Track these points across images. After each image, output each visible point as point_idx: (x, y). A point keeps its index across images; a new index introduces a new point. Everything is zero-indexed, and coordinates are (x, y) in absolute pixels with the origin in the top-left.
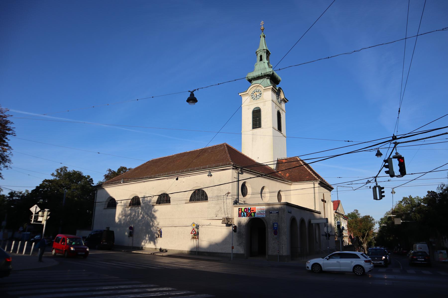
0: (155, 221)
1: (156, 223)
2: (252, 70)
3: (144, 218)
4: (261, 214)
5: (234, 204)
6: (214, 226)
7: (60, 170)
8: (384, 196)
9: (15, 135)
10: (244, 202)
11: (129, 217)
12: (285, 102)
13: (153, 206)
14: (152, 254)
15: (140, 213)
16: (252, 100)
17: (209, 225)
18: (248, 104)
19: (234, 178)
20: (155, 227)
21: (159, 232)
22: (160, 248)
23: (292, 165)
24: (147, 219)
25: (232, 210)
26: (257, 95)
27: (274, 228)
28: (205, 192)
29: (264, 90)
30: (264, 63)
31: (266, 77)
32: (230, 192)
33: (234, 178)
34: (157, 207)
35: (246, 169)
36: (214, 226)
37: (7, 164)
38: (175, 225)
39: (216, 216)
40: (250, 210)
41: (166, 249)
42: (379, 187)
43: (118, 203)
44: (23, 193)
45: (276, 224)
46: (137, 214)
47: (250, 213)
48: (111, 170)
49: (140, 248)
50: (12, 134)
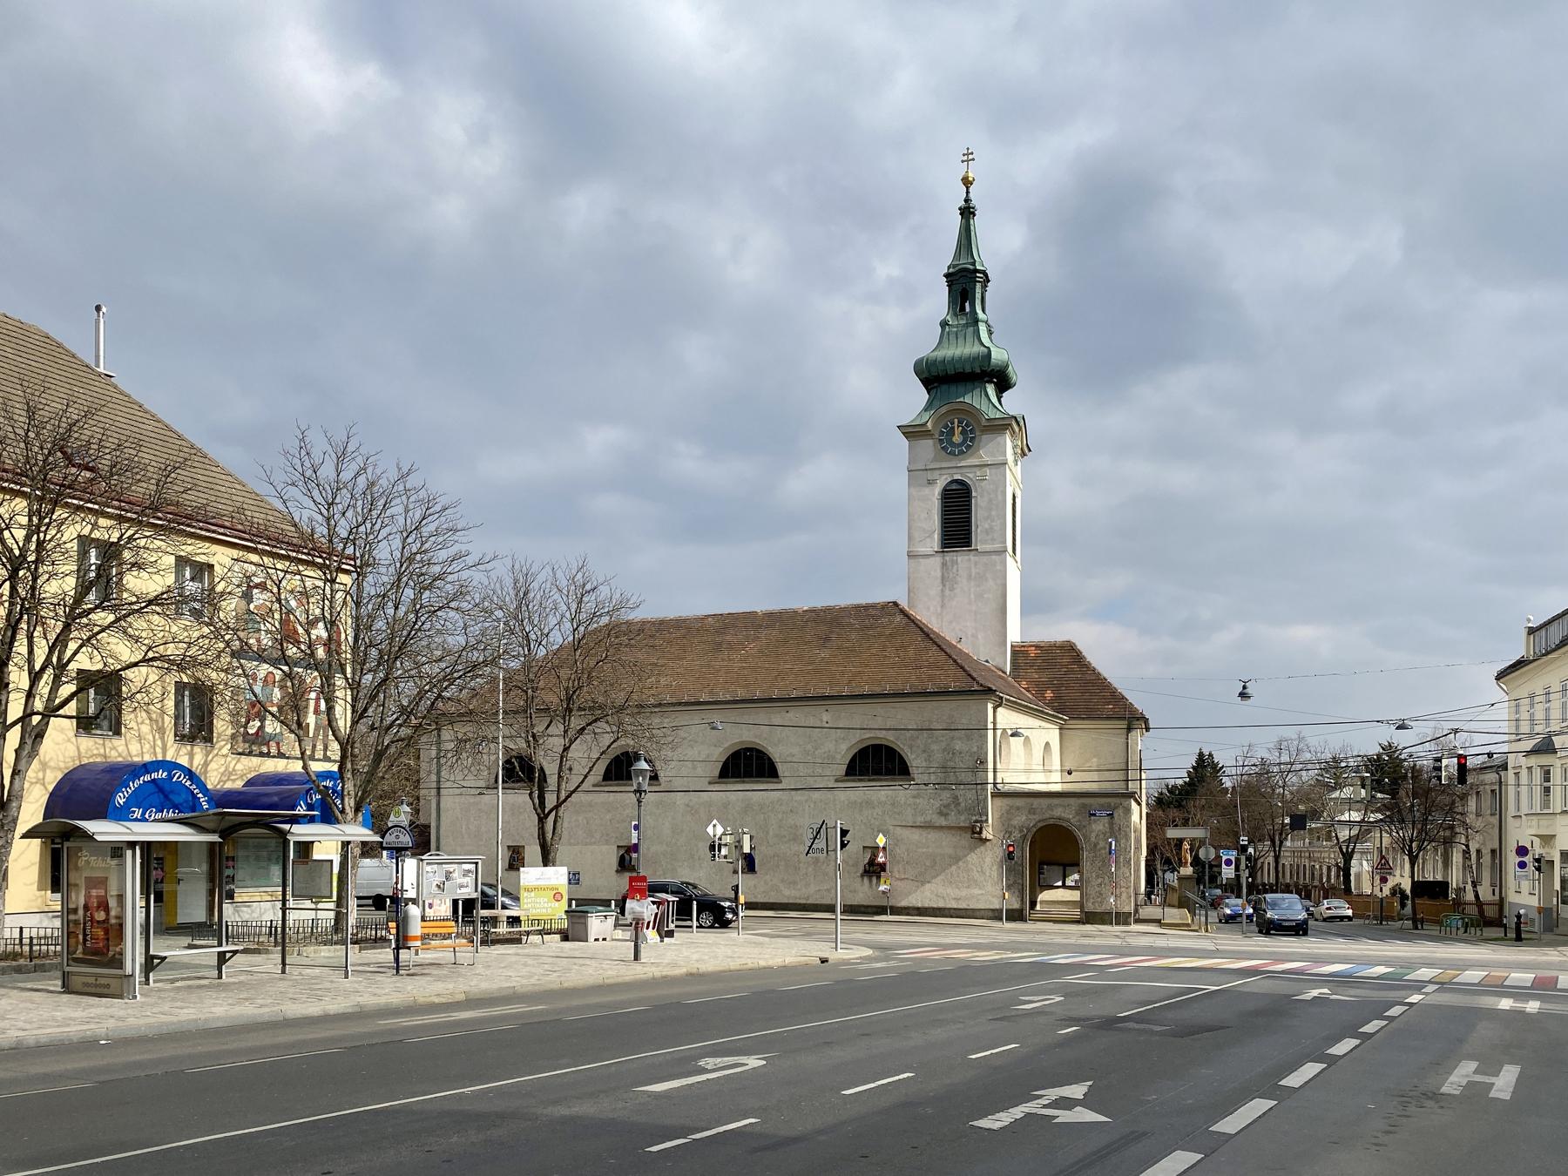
18: (928, 468)
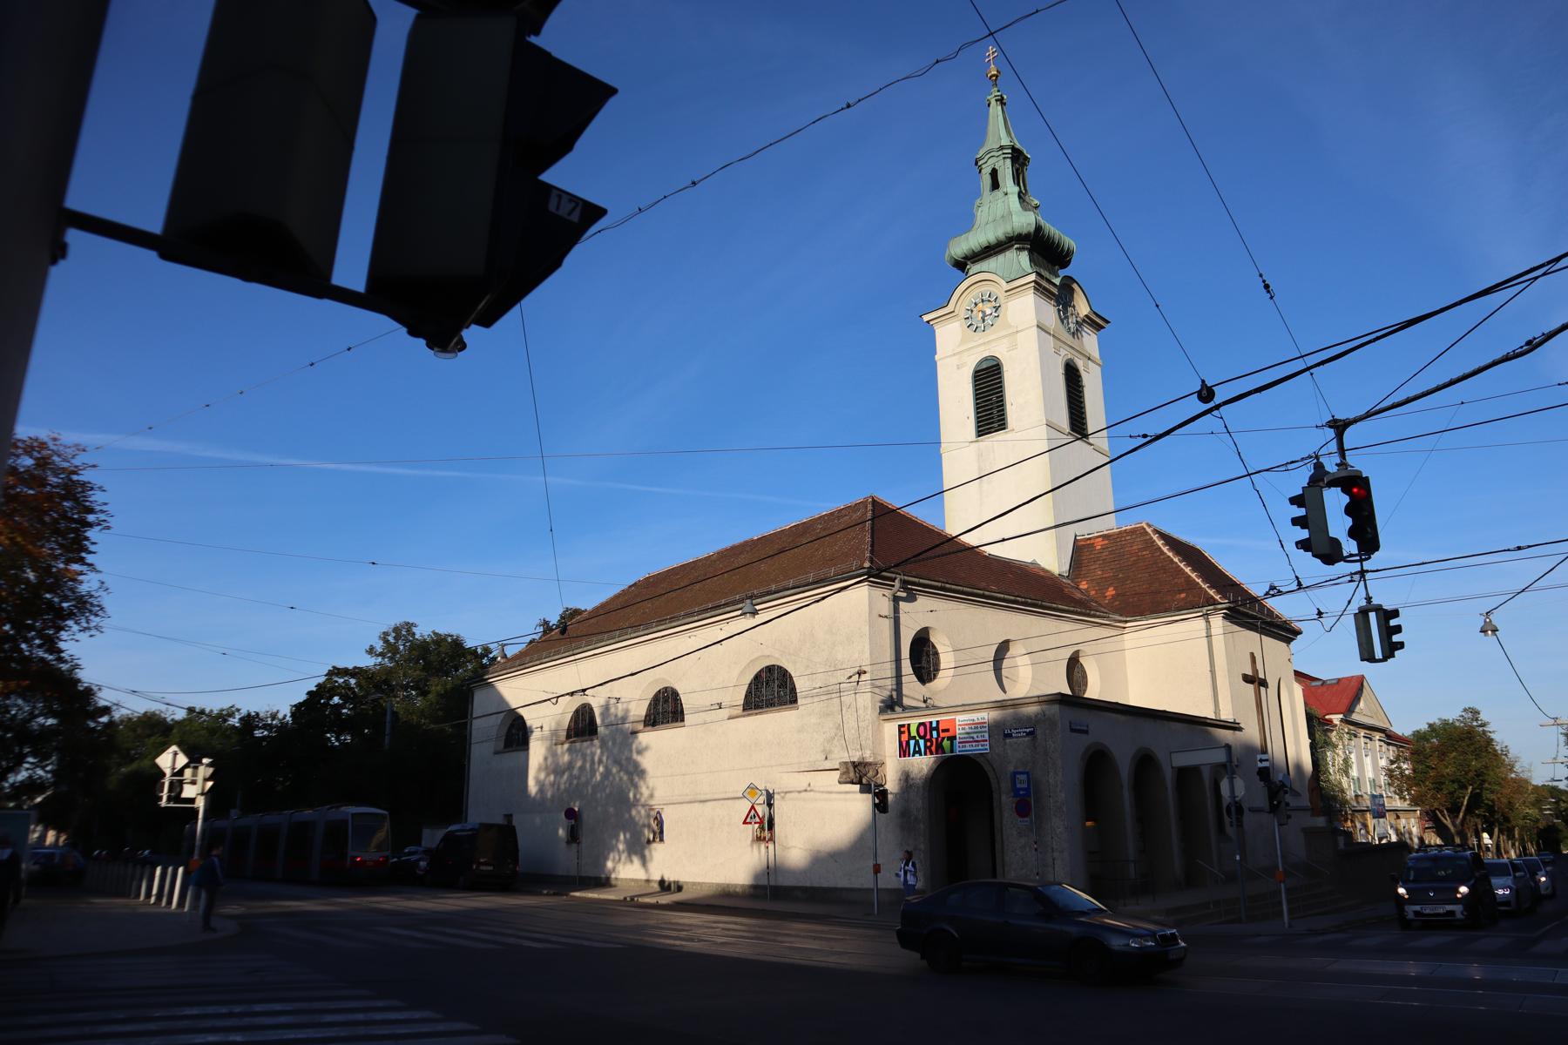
0: (641, 783)
1: (645, 791)
2: (966, 223)
3: (611, 778)
4: (977, 741)
5: (882, 711)
6: (823, 792)
7: (394, 635)
8: (1401, 645)
9: (108, 524)
10: (925, 701)
11: (565, 777)
12: (1099, 328)
13: (634, 733)
14: (628, 899)
15: (596, 759)
16: (970, 332)
17: (806, 791)
19: (880, 616)
20: (643, 806)
21: (656, 822)
22: (659, 878)
23: (1125, 557)
24: (617, 779)
25: (878, 732)
26: (983, 312)
27: (1016, 791)
28: (790, 675)
29: (1008, 293)
30: (1006, 194)
31: (1013, 245)
32: (864, 668)
33: (880, 616)
34: (647, 738)
35: (922, 581)
36: (823, 792)
37: (95, 620)
38: (703, 797)
39: (826, 758)
40: (937, 729)
41: (678, 882)
42: (1378, 609)
43: (532, 732)
44: (280, 716)
45: (1023, 777)
46: (588, 765)
47: (937, 739)
48: (551, 624)
49: (603, 881)
50: (99, 524)
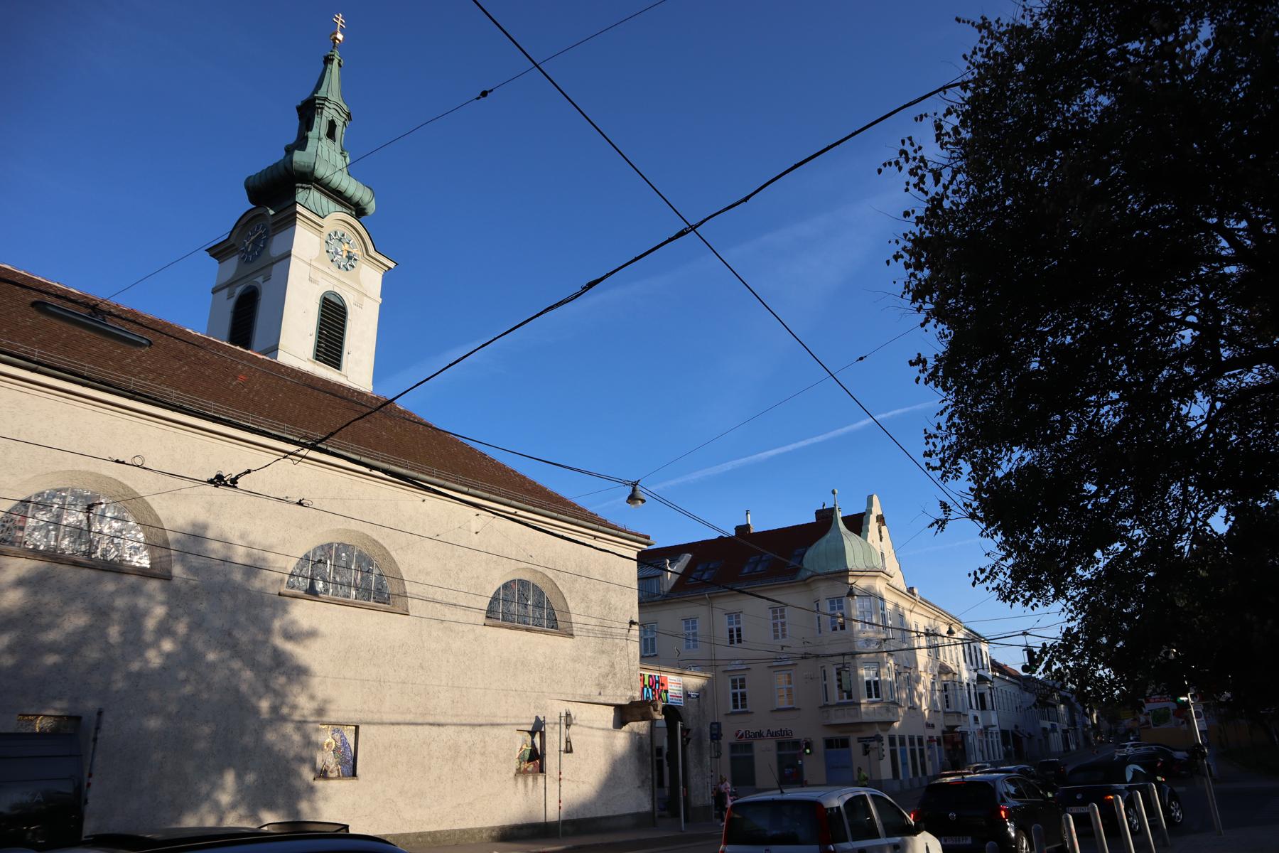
15: (150, 624)
31: (350, 209)
34: (303, 613)
39: (600, 694)
